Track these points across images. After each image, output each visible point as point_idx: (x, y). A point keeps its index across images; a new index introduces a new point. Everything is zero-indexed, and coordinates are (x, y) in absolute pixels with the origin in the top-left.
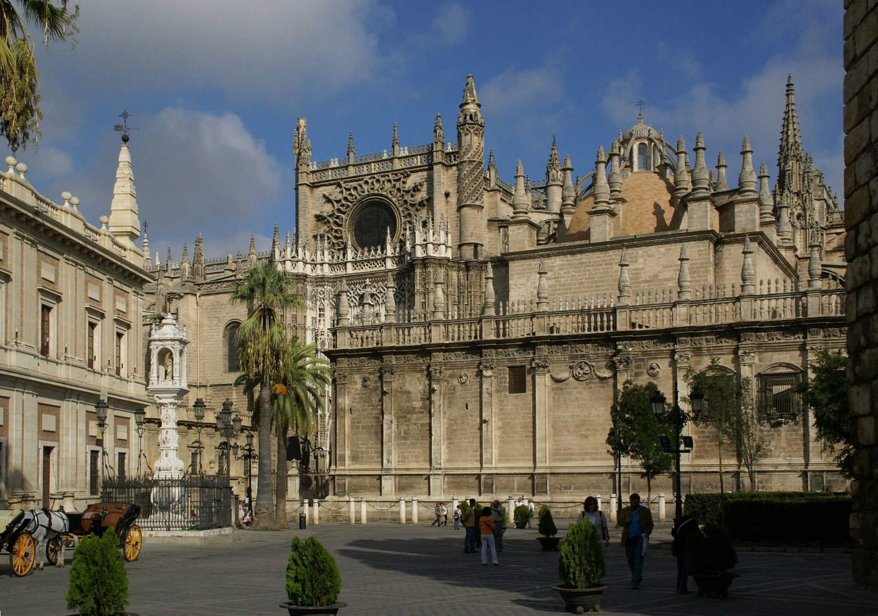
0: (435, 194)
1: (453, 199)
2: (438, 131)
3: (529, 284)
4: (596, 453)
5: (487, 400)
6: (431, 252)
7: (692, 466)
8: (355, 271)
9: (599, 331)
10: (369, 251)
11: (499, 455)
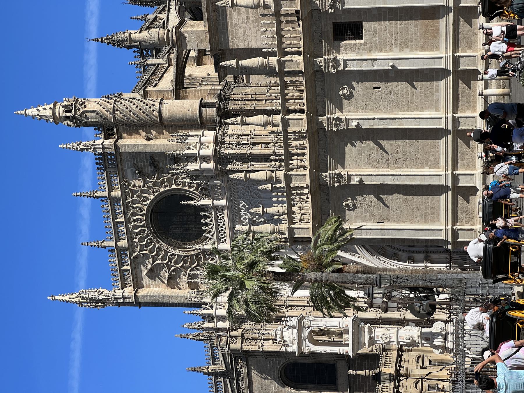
3: (244, 25)
6: (208, 152)
10: (206, 224)
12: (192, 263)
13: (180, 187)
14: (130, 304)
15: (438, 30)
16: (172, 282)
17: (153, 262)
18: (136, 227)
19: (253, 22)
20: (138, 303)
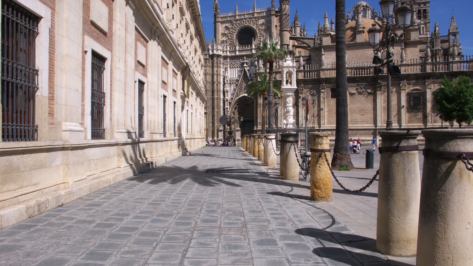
0: (272, 26)
1: (278, 28)
2: (273, 3)
3: (332, 58)
4: (368, 121)
5: (322, 101)
7: (407, 126)
8: (239, 54)
9: (368, 75)
10: (245, 47)
11: (327, 122)
12: (231, 41)
13: (258, 37)
14: (215, 20)
15: (331, 124)
16: (224, 35)
17: (231, 28)
18: (243, 22)
19: (333, 61)
20: (215, 23)
